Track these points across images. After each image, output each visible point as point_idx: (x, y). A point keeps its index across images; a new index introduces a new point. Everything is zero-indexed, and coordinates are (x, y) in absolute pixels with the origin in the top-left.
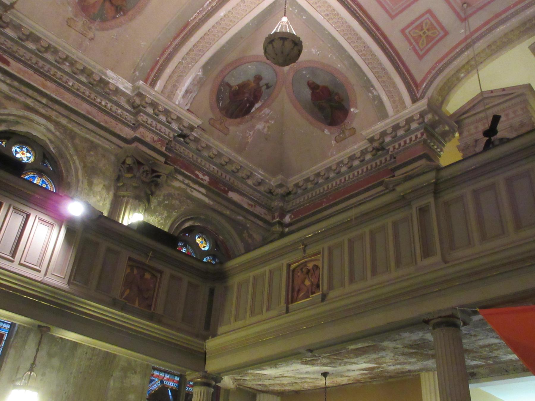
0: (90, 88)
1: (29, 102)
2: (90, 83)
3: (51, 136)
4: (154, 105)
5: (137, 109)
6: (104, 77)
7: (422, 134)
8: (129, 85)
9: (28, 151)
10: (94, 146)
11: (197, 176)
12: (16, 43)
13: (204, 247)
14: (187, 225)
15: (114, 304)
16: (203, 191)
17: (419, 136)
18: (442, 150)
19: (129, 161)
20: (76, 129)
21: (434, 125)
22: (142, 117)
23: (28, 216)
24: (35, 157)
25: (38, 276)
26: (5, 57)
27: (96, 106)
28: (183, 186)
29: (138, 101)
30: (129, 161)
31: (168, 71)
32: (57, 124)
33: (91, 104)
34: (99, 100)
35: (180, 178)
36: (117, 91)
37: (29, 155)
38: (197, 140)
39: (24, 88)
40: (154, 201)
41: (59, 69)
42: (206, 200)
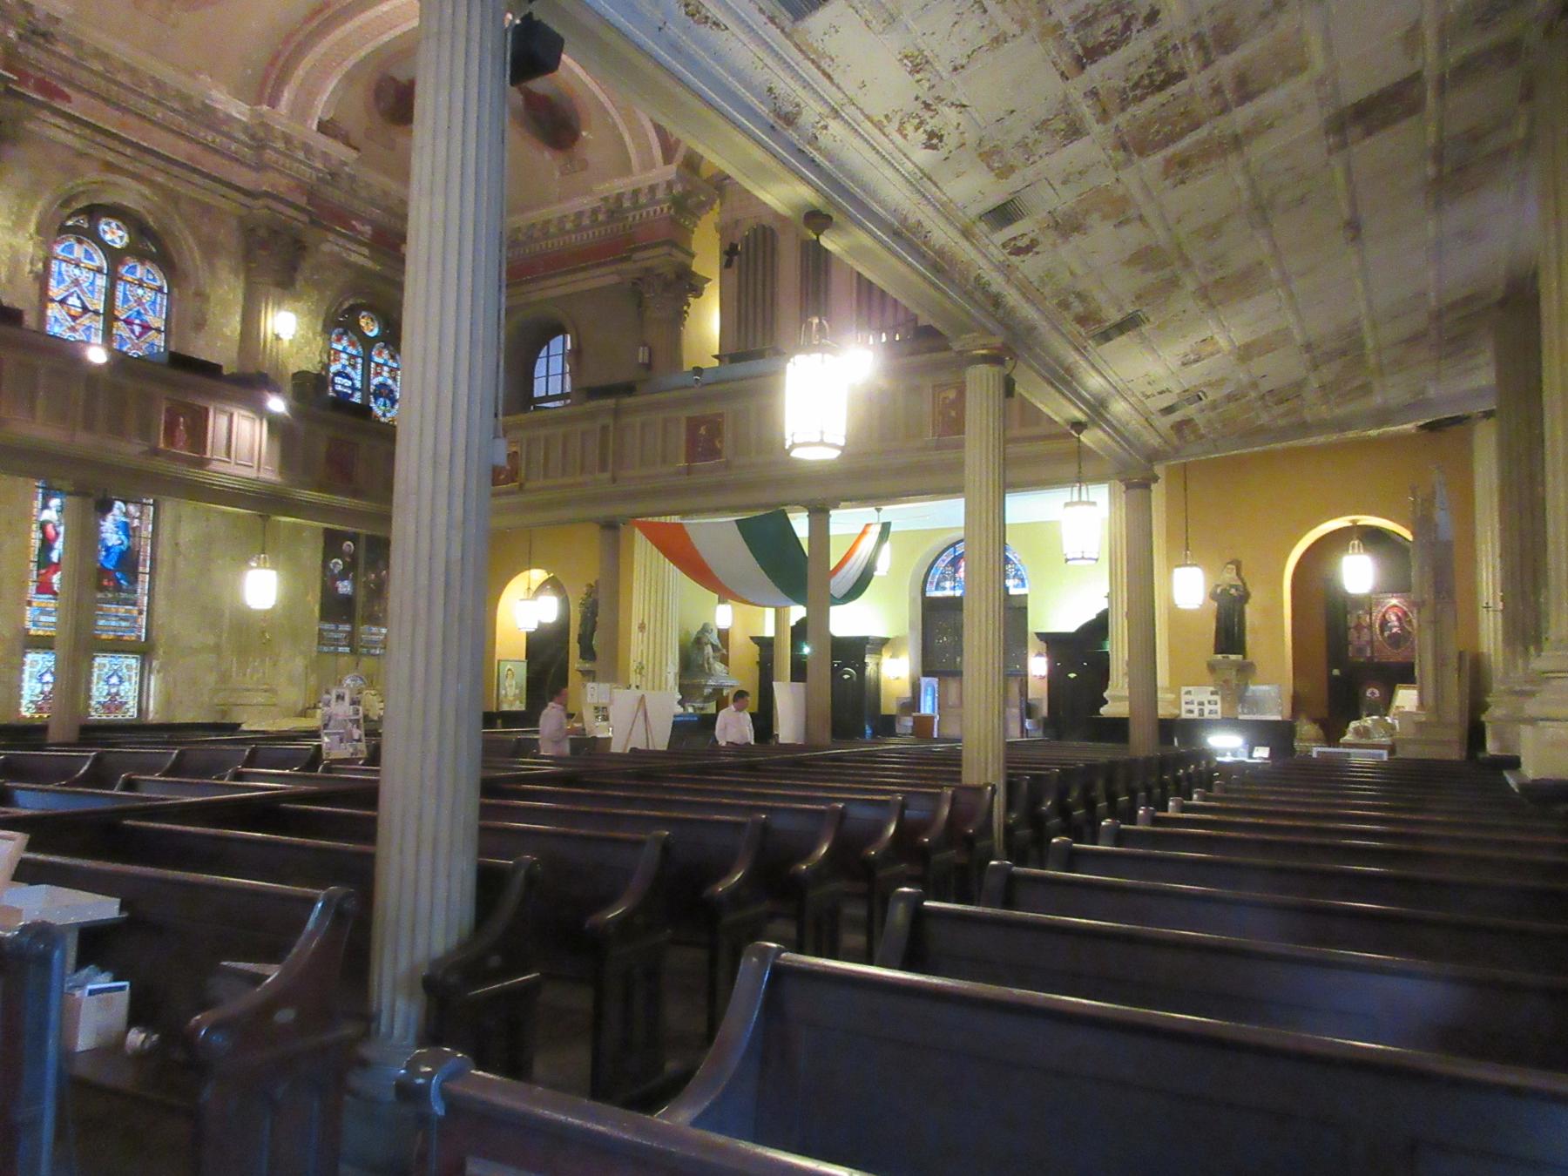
0: (187, 117)
1: (111, 157)
2: (187, 110)
3: (146, 203)
4: (288, 139)
5: (260, 145)
6: (207, 101)
7: (669, 208)
8: (245, 108)
9: (119, 228)
10: (207, 209)
11: (353, 228)
12: (73, 63)
13: (372, 330)
14: (346, 305)
15: (321, 488)
16: (366, 251)
17: (665, 210)
18: (696, 226)
19: (262, 232)
20: (182, 189)
21: (686, 195)
22: (269, 155)
23: (231, 415)
24: (129, 234)
25: (252, 473)
26: (66, 90)
27: (199, 143)
28: (336, 248)
29: (261, 134)
30: (262, 232)
31: (300, 72)
32: (152, 184)
33: (190, 140)
34: (202, 134)
35: (331, 237)
36: (230, 119)
37: (120, 233)
38: (352, 178)
39: (99, 138)
40: (300, 278)
41: (141, 95)
42: (369, 264)
